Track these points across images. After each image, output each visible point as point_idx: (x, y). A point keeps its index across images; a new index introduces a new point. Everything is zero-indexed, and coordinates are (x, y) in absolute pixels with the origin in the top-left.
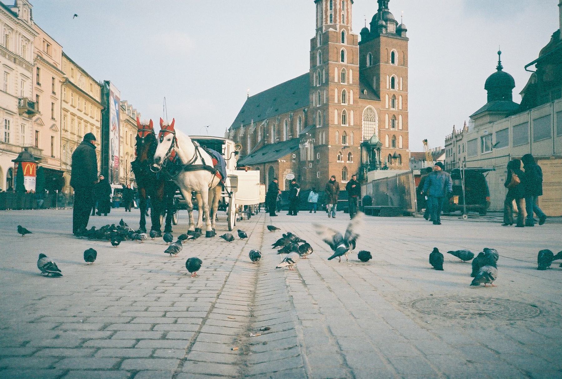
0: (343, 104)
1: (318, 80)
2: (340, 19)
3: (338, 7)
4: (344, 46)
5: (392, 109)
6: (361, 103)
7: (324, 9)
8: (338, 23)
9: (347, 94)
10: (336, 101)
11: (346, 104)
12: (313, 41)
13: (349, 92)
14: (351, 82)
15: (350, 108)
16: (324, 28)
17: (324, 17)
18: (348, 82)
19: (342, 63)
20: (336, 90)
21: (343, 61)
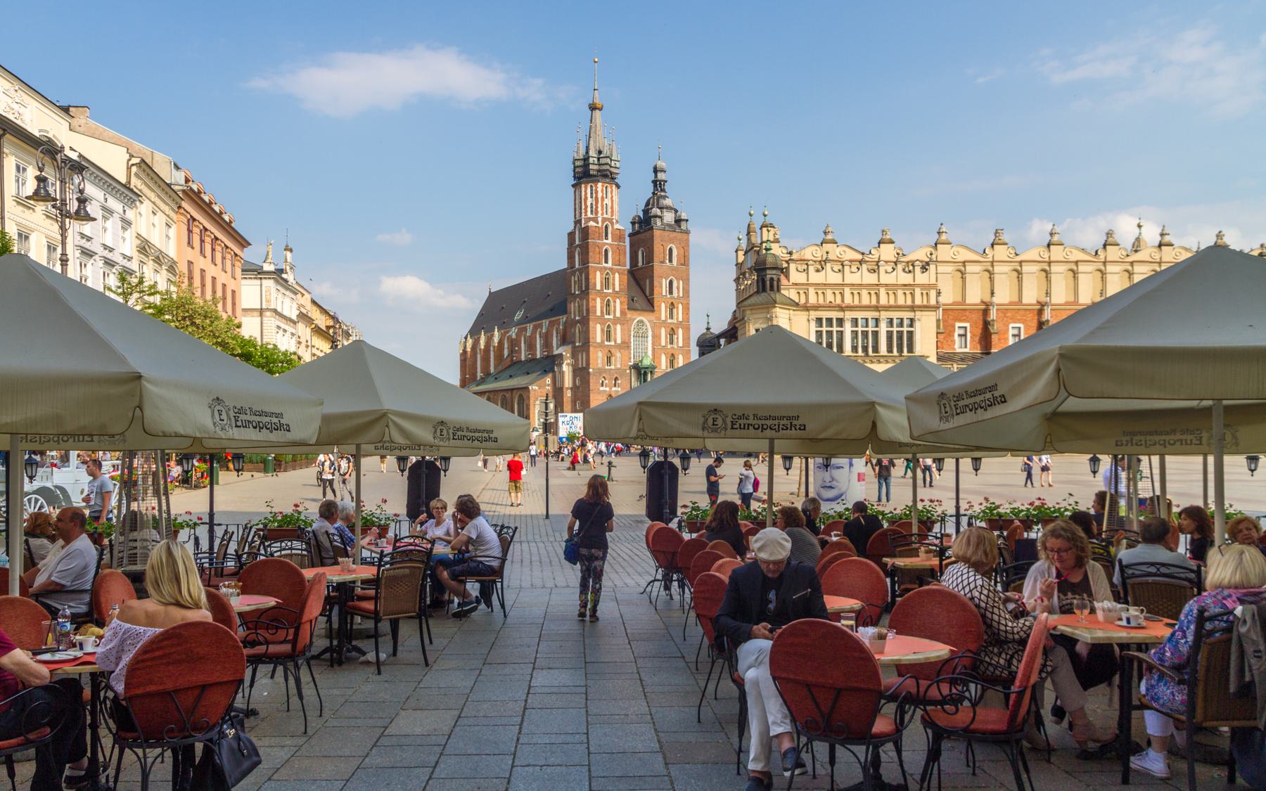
0: (606, 317)
1: (577, 286)
2: (602, 210)
3: (600, 195)
4: (607, 244)
5: (669, 321)
6: (630, 314)
7: (583, 197)
8: (599, 215)
9: (612, 304)
10: (599, 313)
11: (611, 317)
12: (571, 235)
13: (615, 302)
14: (617, 289)
15: (616, 321)
16: (583, 222)
17: (583, 207)
18: (614, 289)
19: (606, 265)
20: (598, 300)
21: (606, 262)
